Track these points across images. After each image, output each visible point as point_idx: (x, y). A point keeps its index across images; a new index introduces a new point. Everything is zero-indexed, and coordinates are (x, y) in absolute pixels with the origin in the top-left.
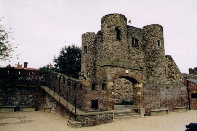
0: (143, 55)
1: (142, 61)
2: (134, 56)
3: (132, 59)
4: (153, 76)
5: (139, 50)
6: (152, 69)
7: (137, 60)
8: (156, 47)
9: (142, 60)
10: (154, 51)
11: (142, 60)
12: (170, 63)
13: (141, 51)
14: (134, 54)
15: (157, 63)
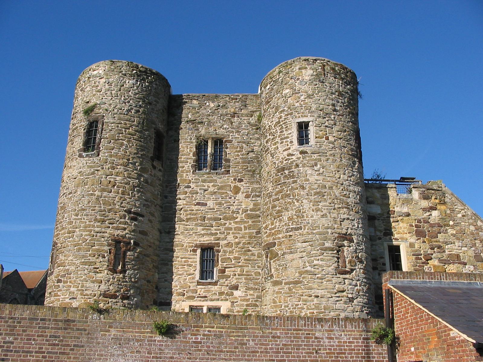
0: (247, 197)
1: (242, 221)
2: (198, 204)
3: (188, 220)
4: (276, 283)
5: (229, 180)
6: (272, 252)
7: (215, 219)
8: (290, 151)
9: (240, 216)
10: (283, 169)
11: (240, 216)
12: (435, 213)
13: (241, 181)
14: (199, 198)
15: (290, 219)
